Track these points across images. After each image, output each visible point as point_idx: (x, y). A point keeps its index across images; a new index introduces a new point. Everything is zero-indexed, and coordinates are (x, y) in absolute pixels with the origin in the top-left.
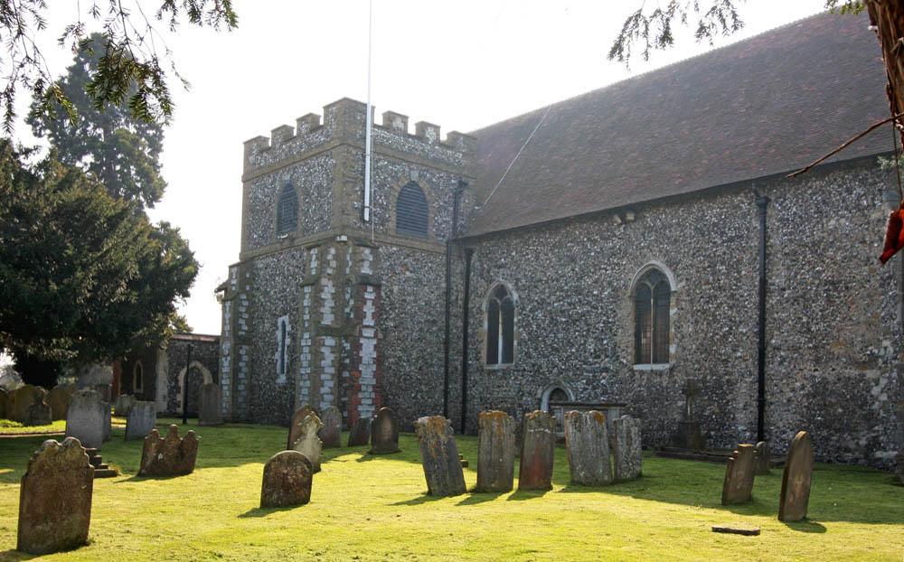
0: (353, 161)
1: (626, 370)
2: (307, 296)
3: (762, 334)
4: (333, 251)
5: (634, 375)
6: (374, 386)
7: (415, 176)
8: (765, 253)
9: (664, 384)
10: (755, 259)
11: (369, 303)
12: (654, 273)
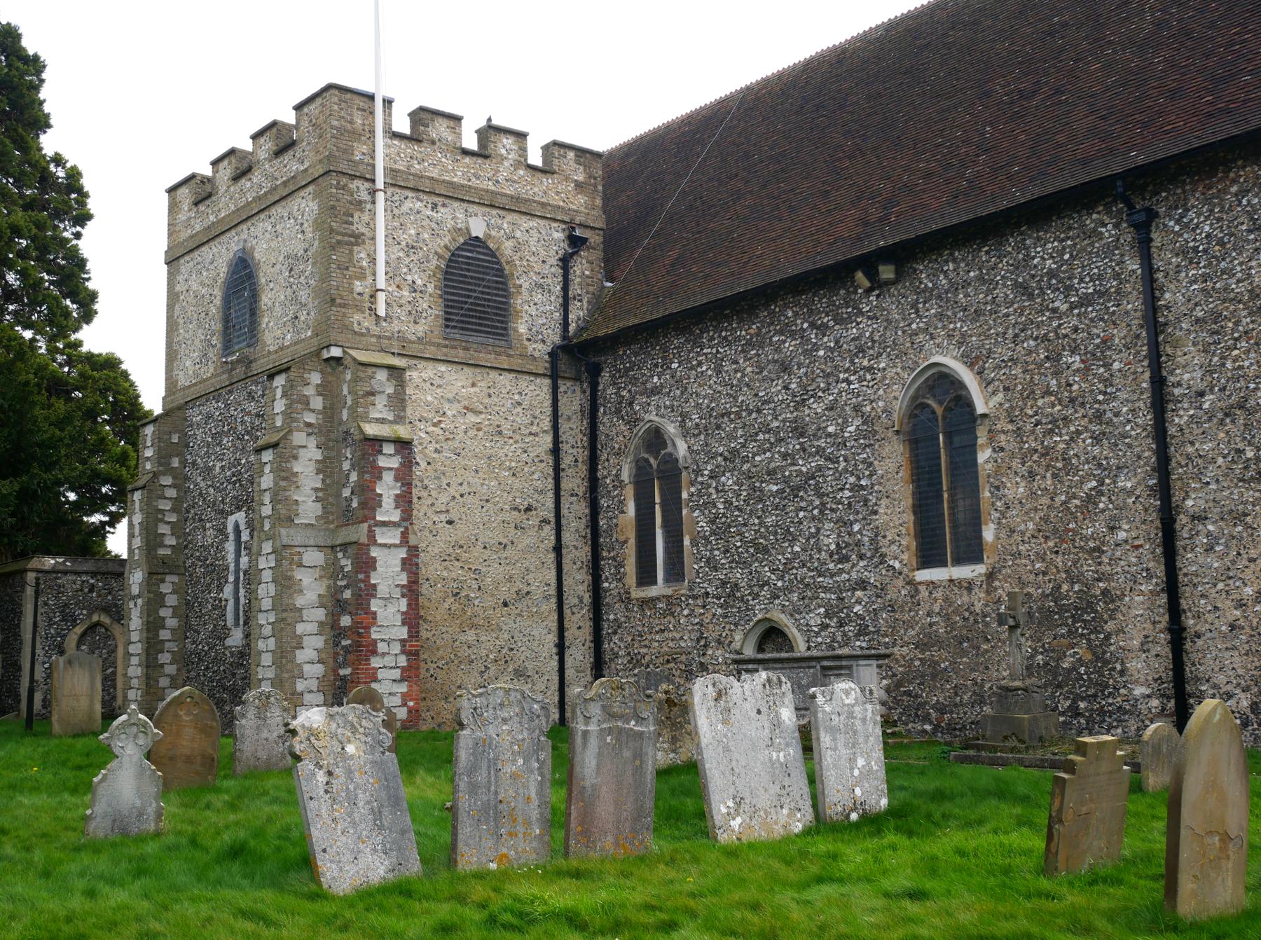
0: (350, 202)
1: (900, 582)
2: (267, 469)
3: (1164, 490)
4: (316, 378)
5: (917, 591)
6: (403, 641)
7: (478, 228)
8: (1154, 322)
9: (978, 607)
10: (1138, 336)
11: (388, 477)
12: (943, 382)
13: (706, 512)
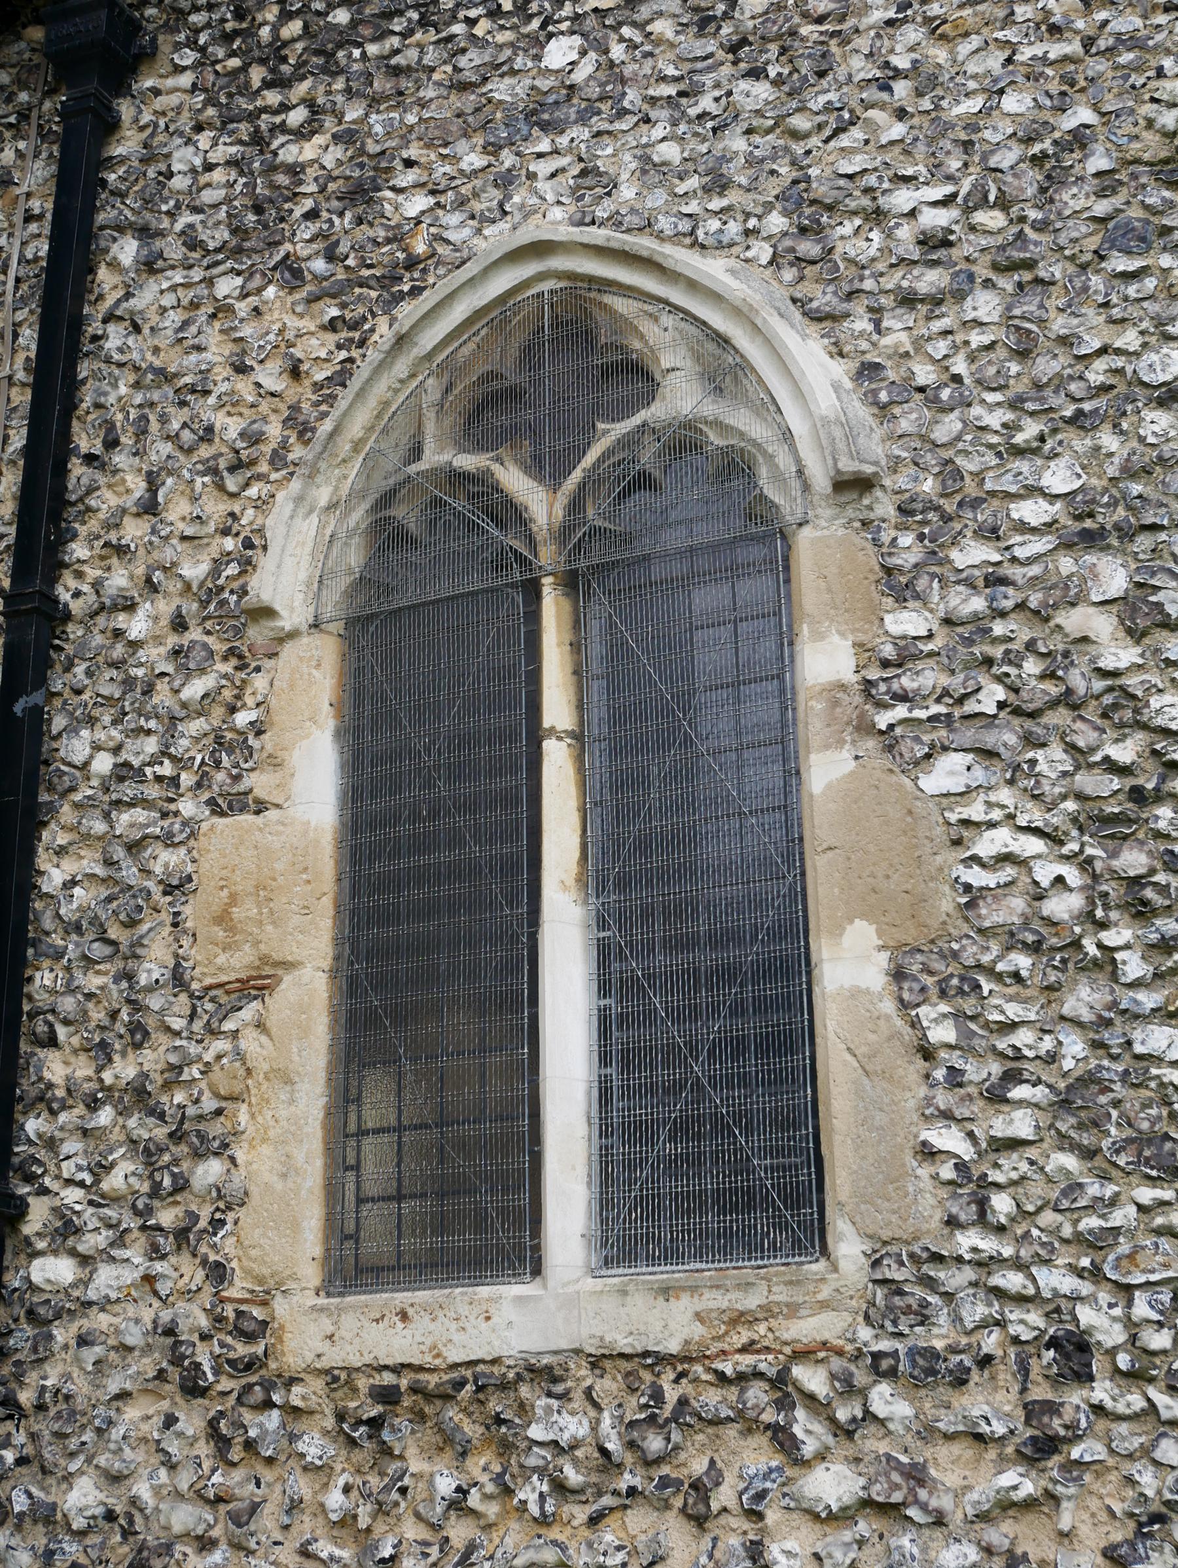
13: (1051, 760)
